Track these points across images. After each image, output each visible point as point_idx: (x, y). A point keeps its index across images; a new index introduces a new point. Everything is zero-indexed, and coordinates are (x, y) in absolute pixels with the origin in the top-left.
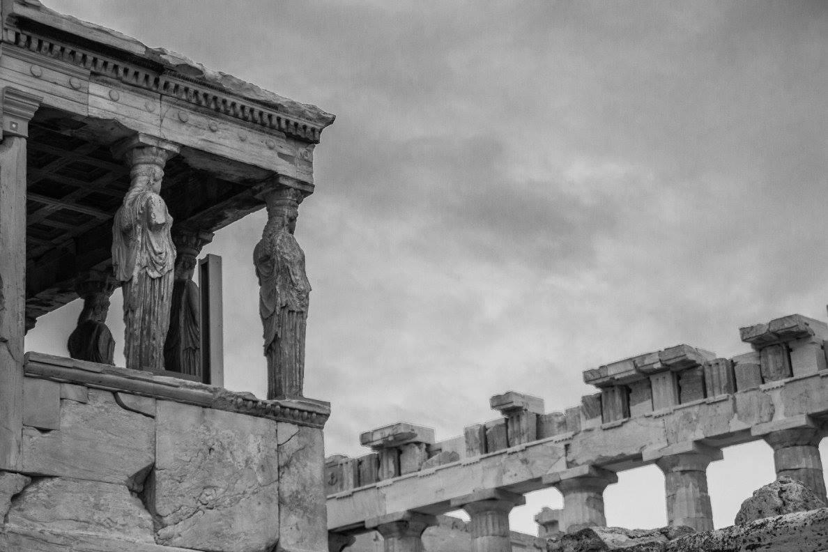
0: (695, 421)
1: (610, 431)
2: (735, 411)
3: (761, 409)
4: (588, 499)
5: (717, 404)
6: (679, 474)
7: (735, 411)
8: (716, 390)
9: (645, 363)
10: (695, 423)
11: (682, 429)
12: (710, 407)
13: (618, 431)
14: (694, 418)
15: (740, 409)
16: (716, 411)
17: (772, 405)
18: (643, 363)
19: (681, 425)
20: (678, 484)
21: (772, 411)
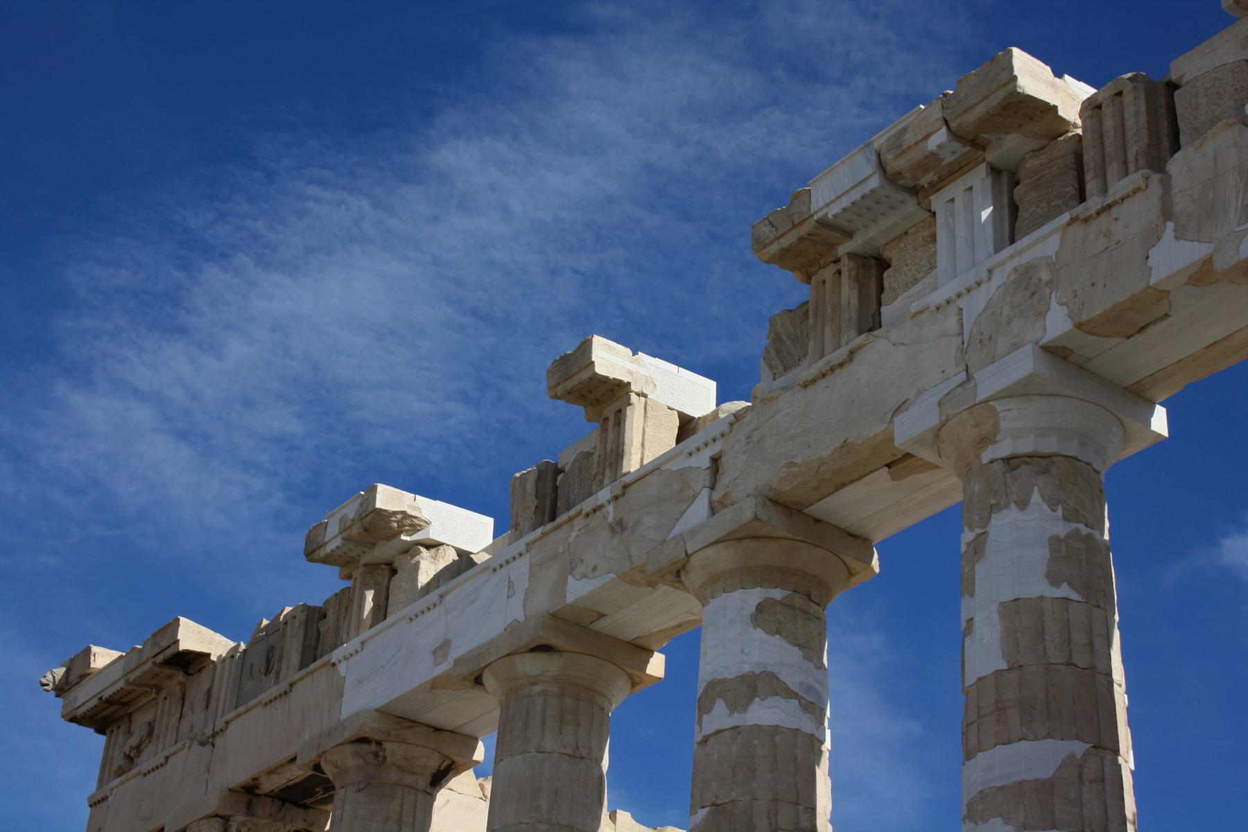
0: (1048, 283)
1: (822, 383)
2: (1167, 213)
4: (760, 608)
5: (1115, 211)
6: (998, 467)
10: (1047, 290)
12: (1094, 226)
13: (841, 377)
14: (1045, 276)
15: (1181, 203)
16: (1108, 235)
19: (1007, 310)
20: (993, 501)
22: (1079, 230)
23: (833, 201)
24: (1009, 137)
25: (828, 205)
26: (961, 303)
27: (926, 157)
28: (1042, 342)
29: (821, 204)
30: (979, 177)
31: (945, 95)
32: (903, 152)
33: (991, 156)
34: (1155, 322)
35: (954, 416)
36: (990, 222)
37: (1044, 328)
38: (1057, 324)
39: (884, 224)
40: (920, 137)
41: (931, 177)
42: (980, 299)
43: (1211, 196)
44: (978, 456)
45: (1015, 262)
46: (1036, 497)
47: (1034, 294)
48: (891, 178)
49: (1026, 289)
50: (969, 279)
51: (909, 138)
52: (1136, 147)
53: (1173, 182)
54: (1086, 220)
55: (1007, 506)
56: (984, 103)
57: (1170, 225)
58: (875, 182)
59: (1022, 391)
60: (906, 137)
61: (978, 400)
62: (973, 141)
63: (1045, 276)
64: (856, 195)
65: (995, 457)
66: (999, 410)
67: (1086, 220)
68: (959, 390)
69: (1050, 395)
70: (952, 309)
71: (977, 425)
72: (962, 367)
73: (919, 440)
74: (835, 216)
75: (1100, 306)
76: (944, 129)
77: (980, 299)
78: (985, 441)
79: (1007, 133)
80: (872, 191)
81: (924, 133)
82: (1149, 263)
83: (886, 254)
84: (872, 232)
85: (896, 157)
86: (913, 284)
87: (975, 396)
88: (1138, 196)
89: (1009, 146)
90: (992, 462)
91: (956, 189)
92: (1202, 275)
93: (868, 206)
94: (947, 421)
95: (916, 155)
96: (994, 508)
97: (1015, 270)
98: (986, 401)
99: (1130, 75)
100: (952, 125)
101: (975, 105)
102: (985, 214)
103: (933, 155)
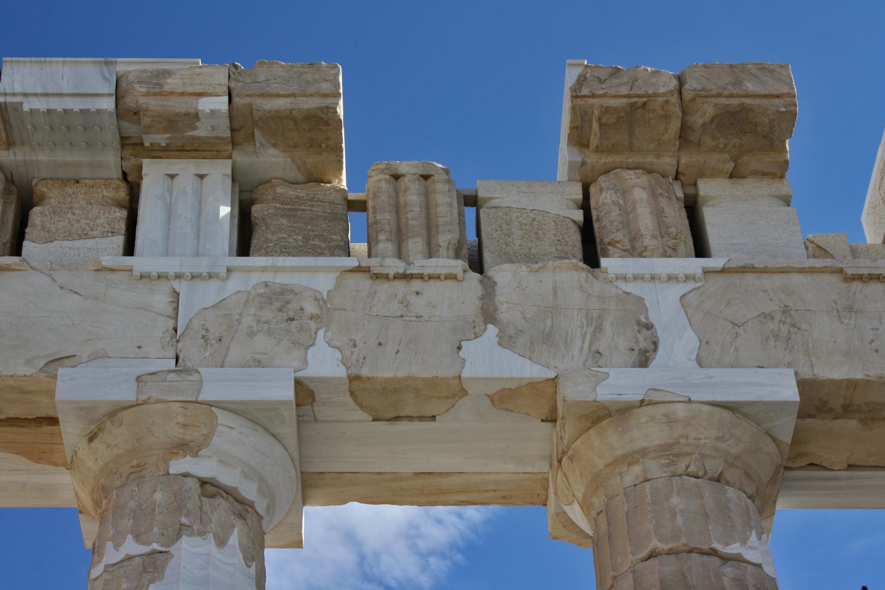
0: (312, 317)
3: (599, 329)
5: (416, 285)
6: (193, 485)
7: (489, 316)
8: (415, 245)
9: (167, 88)
10: (313, 325)
11: (251, 334)
12: (384, 288)
14: (310, 308)
15: (505, 313)
17: (649, 327)
18: (161, 85)
19: (248, 321)
20: (184, 520)
21: (643, 344)
22: (364, 283)
23: (36, 95)
24: (272, 151)
25: (25, 95)
26: (182, 287)
27: (187, 114)
28: (300, 374)
29: (18, 89)
30: (219, 172)
31: (236, 67)
32: (160, 94)
33: (240, 157)
34: (410, 418)
35: (158, 401)
36: (228, 221)
37: (305, 362)
38: (324, 362)
39: (61, 156)
40: (191, 90)
41: (161, 139)
42: (208, 294)
43: (549, 323)
44: (166, 461)
45: (268, 277)
46: (234, 539)
47: (292, 319)
48: (123, 112)
49: (280, 310)
50: (202, 265)
51: (172, 83)
52: (449, 236)
53: (499, 290)
54: (377, 277)
55: (202, 534)
56: (289, 100)
57: (492, 330)
58: (108, 104)
59: (253, 414)
60: (169, 81)
61: (202, 397)
62: (242, 127)
63: (310, 308)
64: (76, 105)
65: (193, 471)
66: (220, 421)
67: (377, 277)
68: (172, 376)
69: (273, 435)
70: (165, 286)
71: (185, 426)
72: (171, 353)
73: (86, 409)
74: (31, 110)
75: (387, 369)
76: (226, 98)
77: (208, 294)
78: (183, 448)
79: (274, 145)
80: (99, 111)
81: (198, 89)
82: (461, 353)
83: (42, 188)
84: (43, 157)
85: (148, 94)
86: (80, 238)
87: (199, 391)
88: (450, 283)
89: (270, 160)
90: (186, 475)
91: (186, 169)
92: (506, 397)
93: (67, 126)
94: (145, 403)
95: (177, 105)
96: (180, 531)
97: (266, 285)
98: (210, 404)
99: (440, 166)
100: (236, 100)
101: (278, 96)
102: (225, 210)
103: (195, 117)
